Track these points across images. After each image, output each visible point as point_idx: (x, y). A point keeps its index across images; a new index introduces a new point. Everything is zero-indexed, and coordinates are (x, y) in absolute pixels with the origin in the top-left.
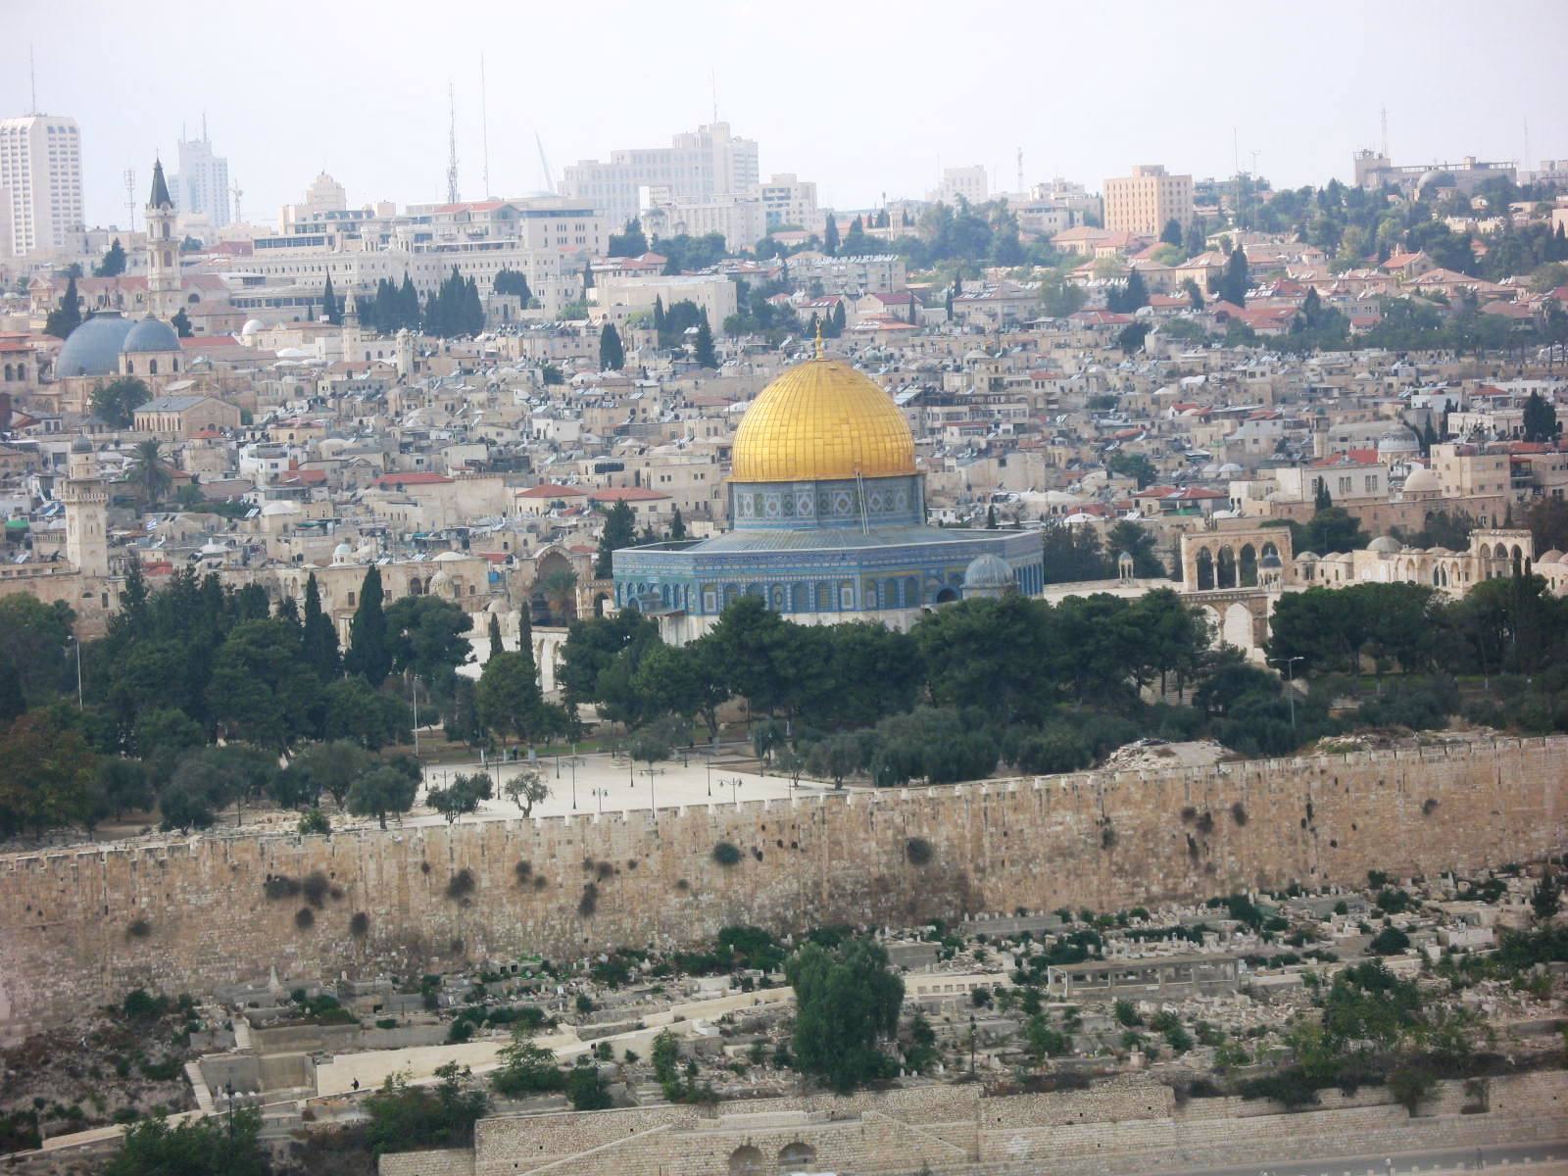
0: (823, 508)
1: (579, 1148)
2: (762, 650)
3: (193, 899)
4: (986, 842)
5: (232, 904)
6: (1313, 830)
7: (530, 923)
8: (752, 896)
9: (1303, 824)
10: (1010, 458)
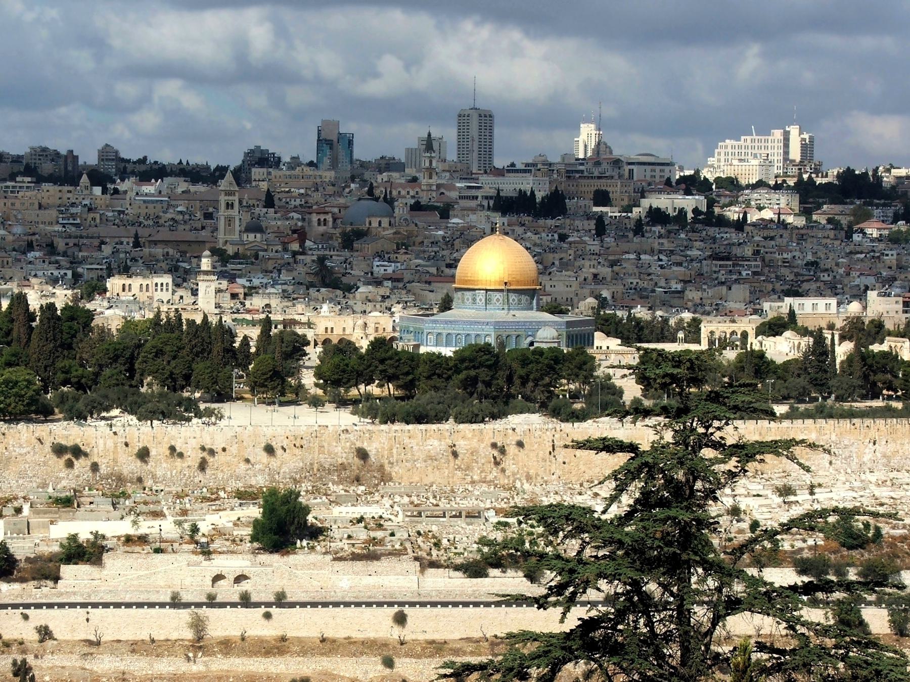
0: (488, 301)
1: (147, 569)
2: (382, 361)
3: (17, 450)
4: (395, 451)
5: (35, 453)
6: (555, 456)
7: (174, 472)
8: (280, 468)
9: (550, 453)
10: (735, 287)
